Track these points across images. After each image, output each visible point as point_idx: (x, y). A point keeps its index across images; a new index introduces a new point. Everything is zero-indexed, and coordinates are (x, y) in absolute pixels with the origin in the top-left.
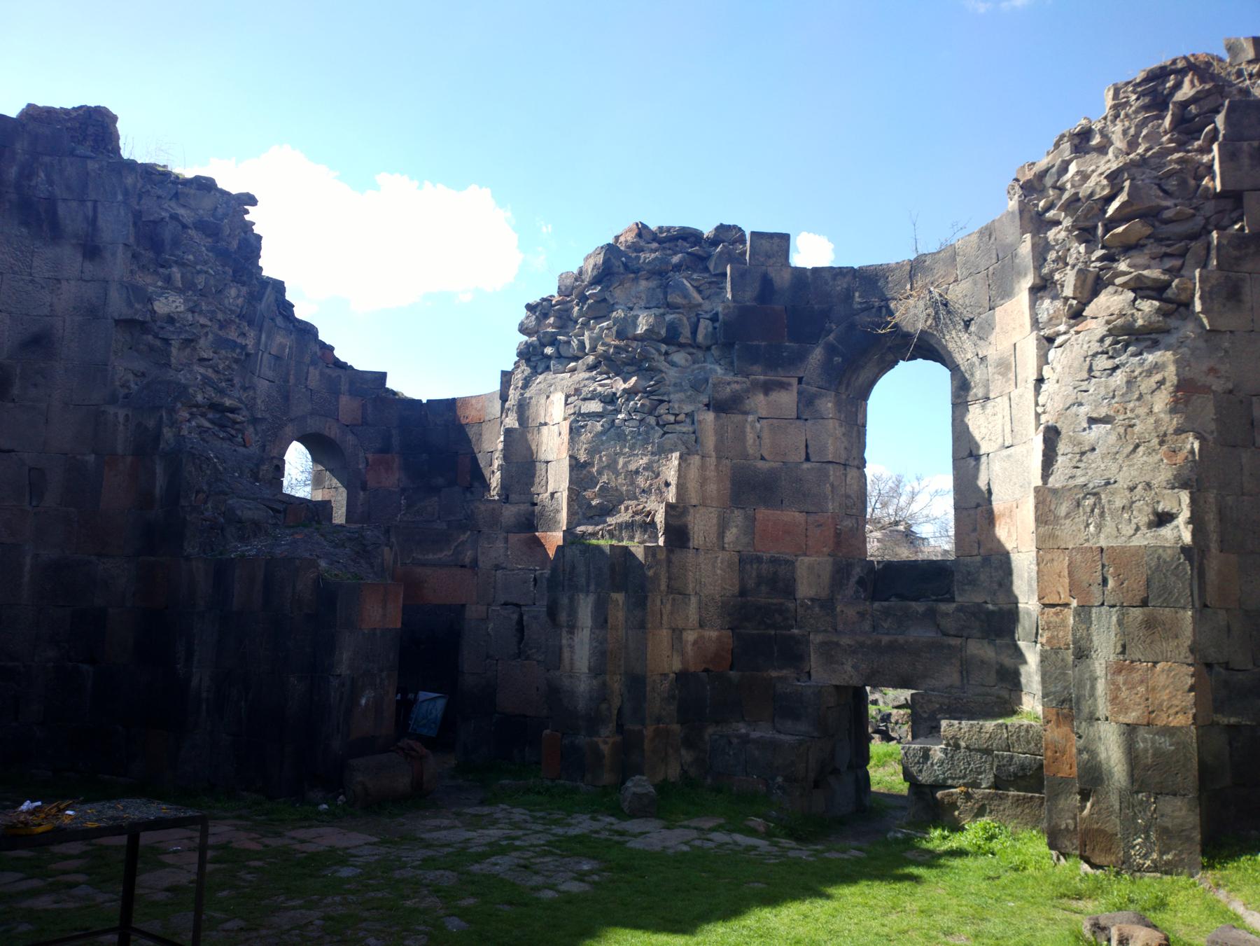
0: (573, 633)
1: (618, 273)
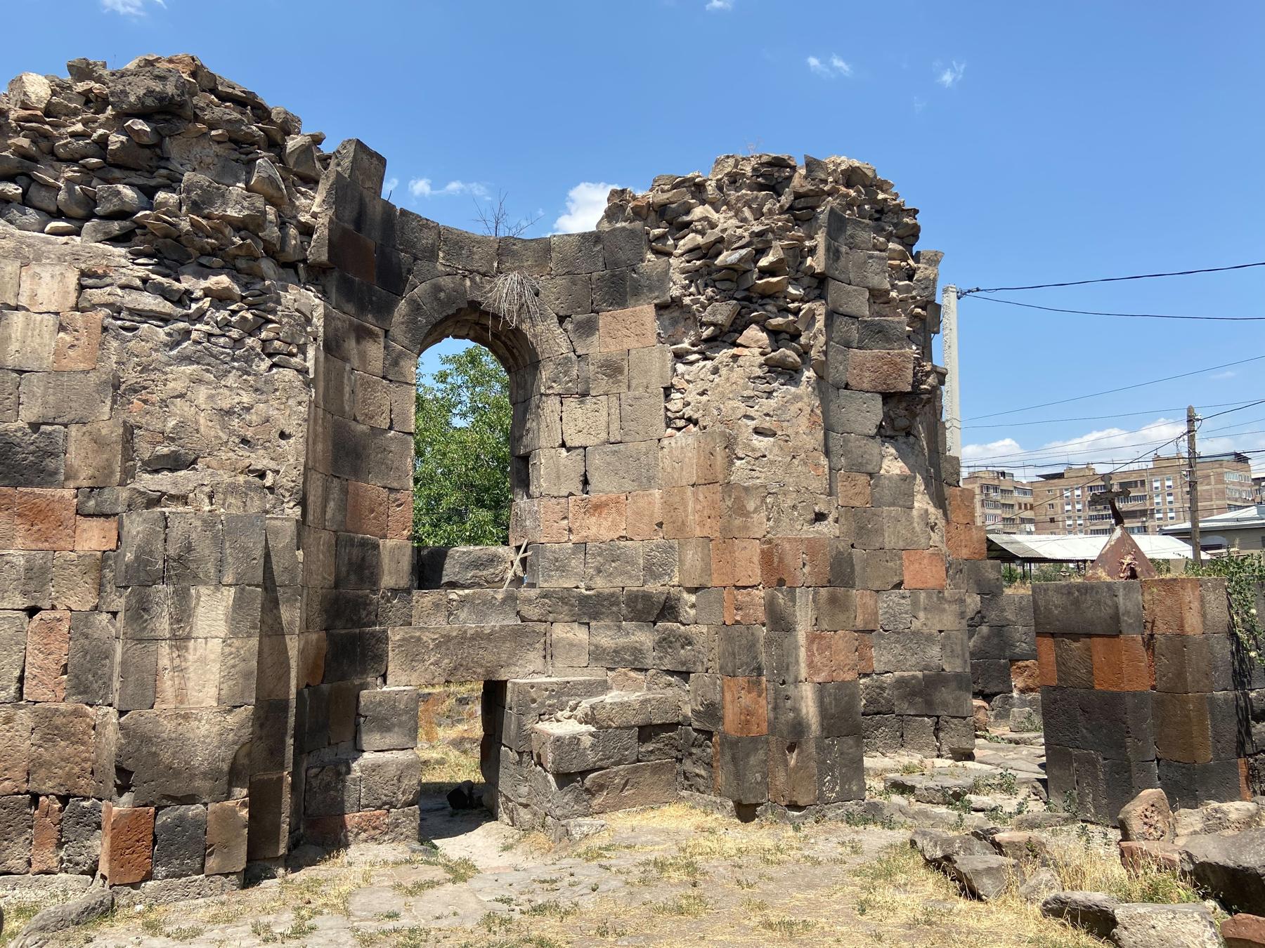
0: (186, 648)
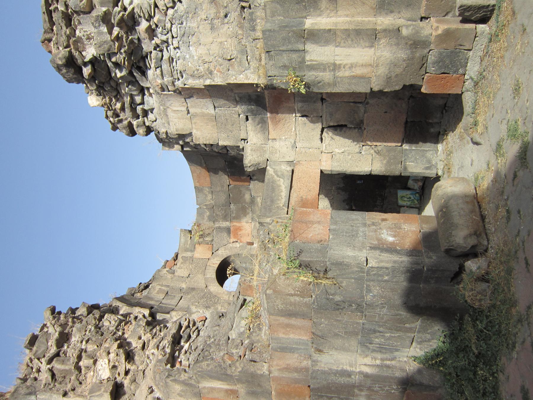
0: (340, 65)
1: (70, 52)
